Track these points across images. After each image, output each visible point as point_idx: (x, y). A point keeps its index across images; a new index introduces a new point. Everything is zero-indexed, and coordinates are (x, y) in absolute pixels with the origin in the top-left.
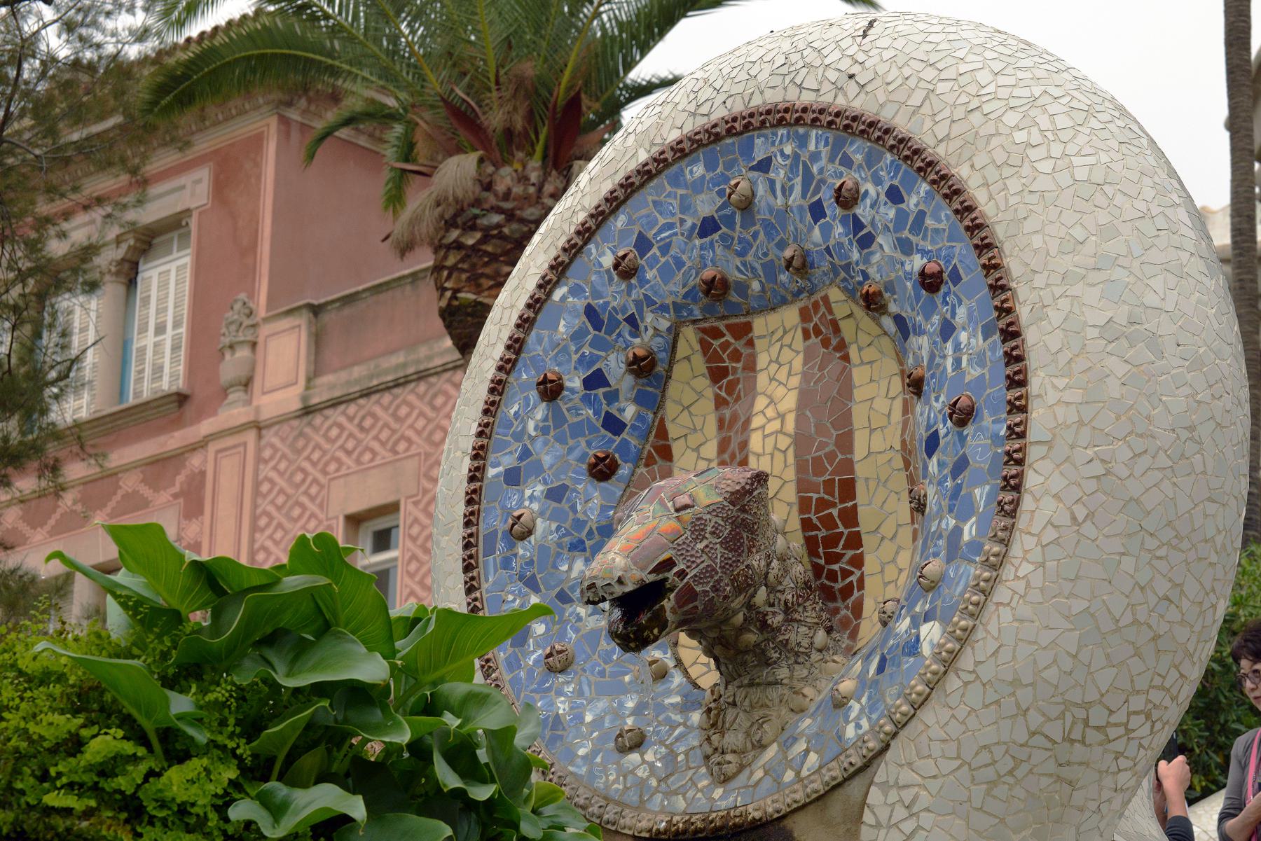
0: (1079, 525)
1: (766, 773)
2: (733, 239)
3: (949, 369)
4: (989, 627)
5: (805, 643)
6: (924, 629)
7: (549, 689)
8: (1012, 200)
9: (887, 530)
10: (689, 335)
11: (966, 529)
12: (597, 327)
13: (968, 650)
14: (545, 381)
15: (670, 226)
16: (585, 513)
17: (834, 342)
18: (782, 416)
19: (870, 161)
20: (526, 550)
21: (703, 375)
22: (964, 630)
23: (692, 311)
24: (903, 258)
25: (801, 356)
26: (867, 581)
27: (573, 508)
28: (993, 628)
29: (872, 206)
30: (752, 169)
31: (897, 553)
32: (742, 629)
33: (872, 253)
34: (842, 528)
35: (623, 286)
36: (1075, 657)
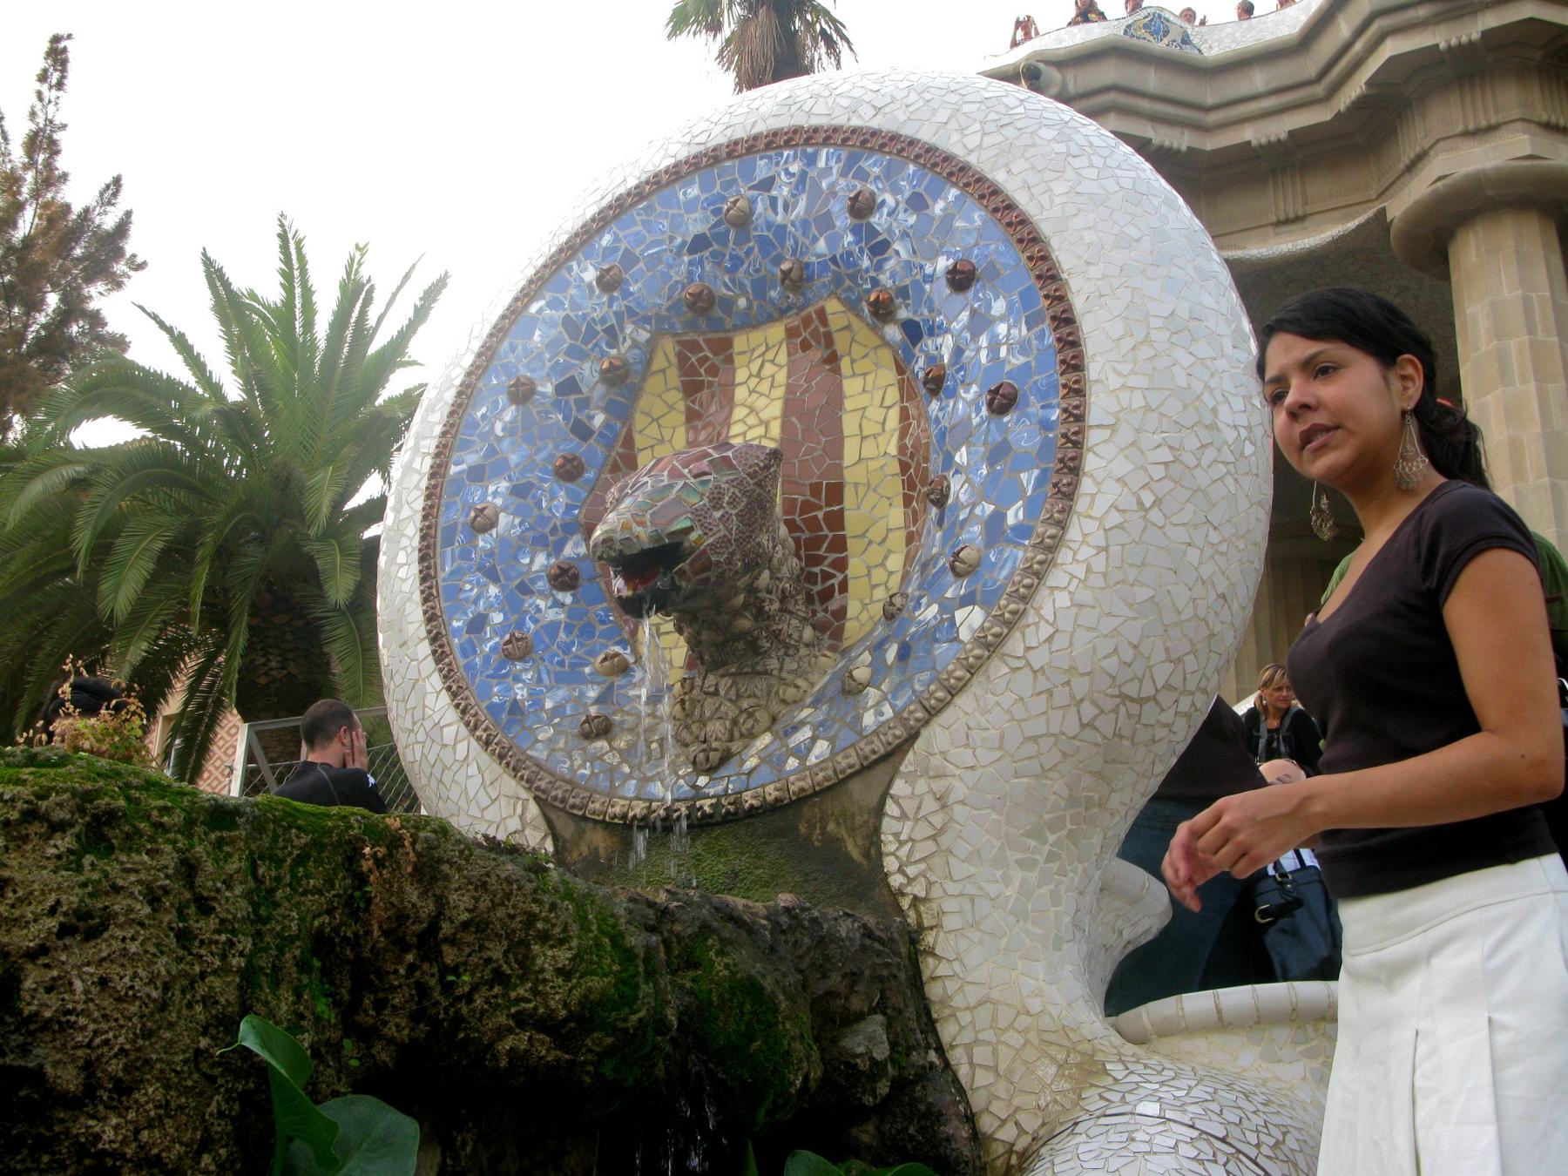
0: (1146, 510)
1: (763, 760)
5: (795, 636)
6: (959, 615)
7: (506, 676)
8: (1058, 200)
9: (876, 534)
10: (669, 347)
11: (1010, 514)
12: (573, 336)
13: (1017, 635)
14: (517, 385)
16: (550, 510)
18: (767, 424)
19: (889, 174)
22: (1013, 613)
25: (785, 370)
26: (851, 584)
27: (539, 504)
28: (1047, 612)
29: (889, 214)
31: (886, 557)
32: (736, 614)
33: (887, 259)
34: (826, 531)
35: (605, 299)
36: (1136, 647)
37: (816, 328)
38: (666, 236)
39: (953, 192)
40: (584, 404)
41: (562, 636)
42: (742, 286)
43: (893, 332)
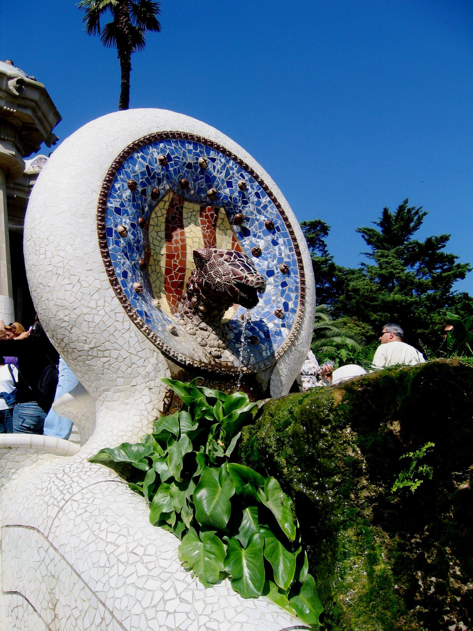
3: (277, 255)
6: (283, 329)
10: (171, 194)
12: (149, 174)
15: (179, 158)
24: (257, 214)
30: (208, 158)
33: (246, 207)
39: (268, 199)
40: (146, 200)
42: (195, 187)
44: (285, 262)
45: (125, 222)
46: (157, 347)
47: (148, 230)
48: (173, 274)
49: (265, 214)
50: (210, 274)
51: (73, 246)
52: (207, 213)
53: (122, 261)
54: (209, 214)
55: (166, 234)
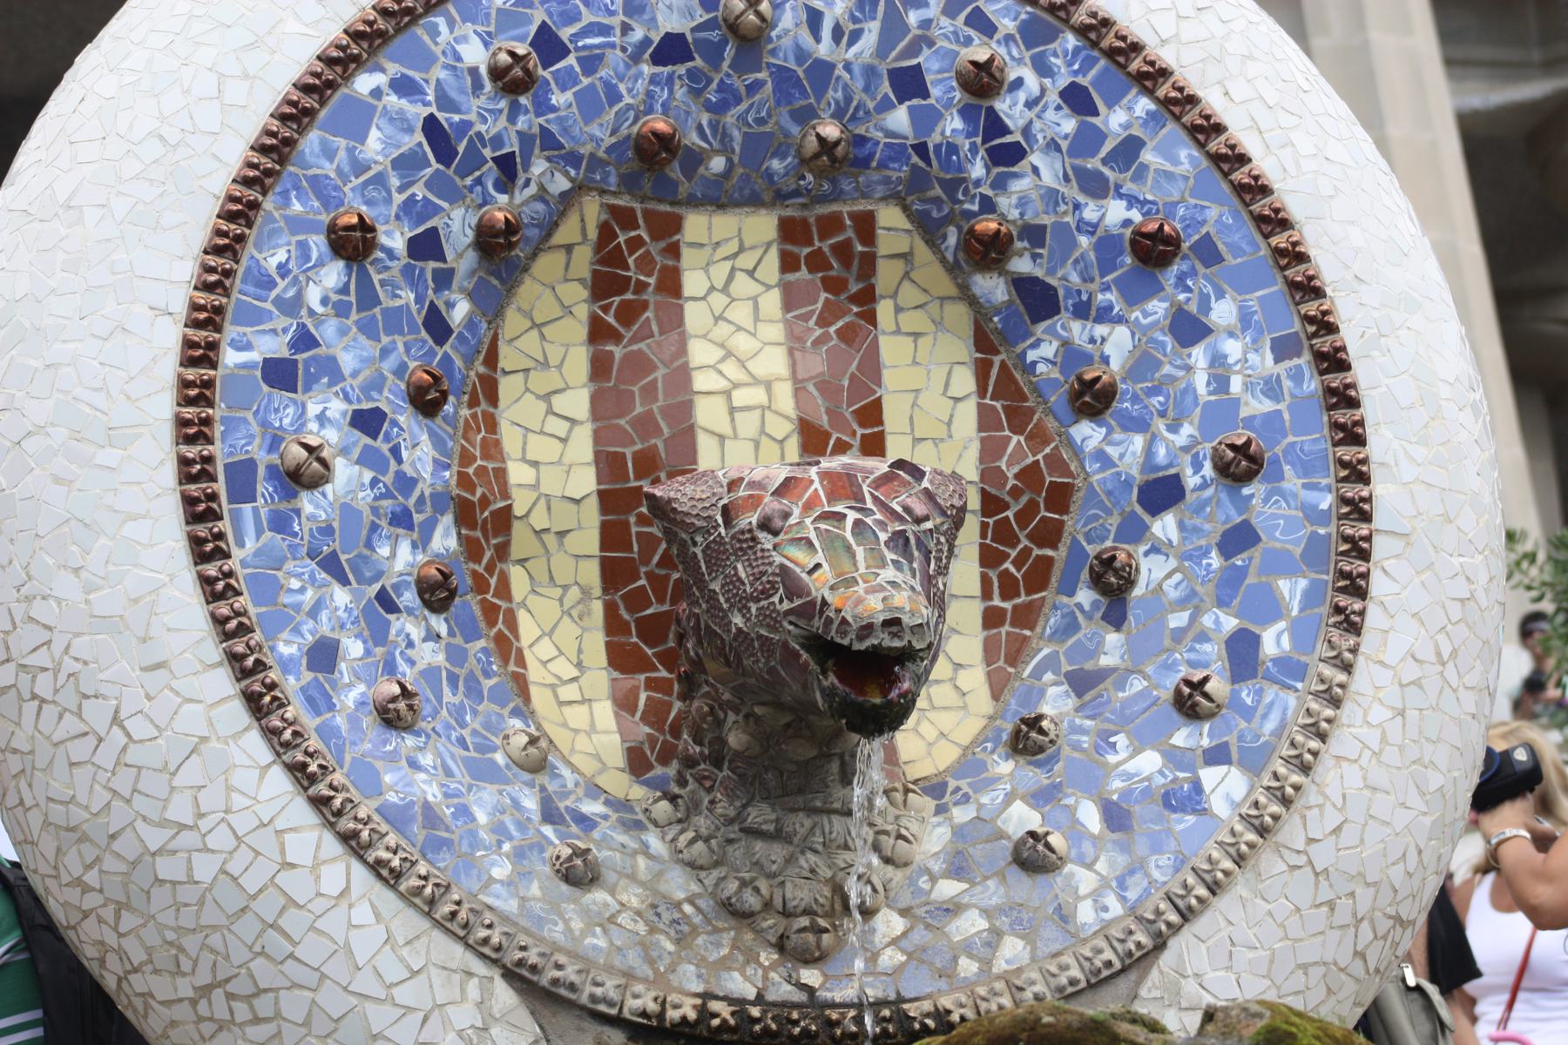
2: (710, 81)
4: (1328, 791)
6: (1210, 776)
10: (592, 210)
13: (1297, 819)
15: (605, 30)
16: (413, 464)
17: (854, 287)
18: (768, 386)
20: (317, 506)
21: (581, 281)
23: (607, 175)
24: (1081, 199)
27: (395, 451)
33: (1016, 176)
35: (503, 104)
37: (848, 242)
38: (615, 21)
39: (1144, 105)
41: (448, 696)
42: (725, 137)
43: (993, 288)
44: (1248, 422)
45: (322, 419)
46: (483, 956)
47: (493, 399)
48: (642, 582)
49: (1129, 187)
50: (712, 596)
51: (83, 574)
52: (817, 243)
53: (309, 596)
54: (826, 250)
55: (595, 399)
